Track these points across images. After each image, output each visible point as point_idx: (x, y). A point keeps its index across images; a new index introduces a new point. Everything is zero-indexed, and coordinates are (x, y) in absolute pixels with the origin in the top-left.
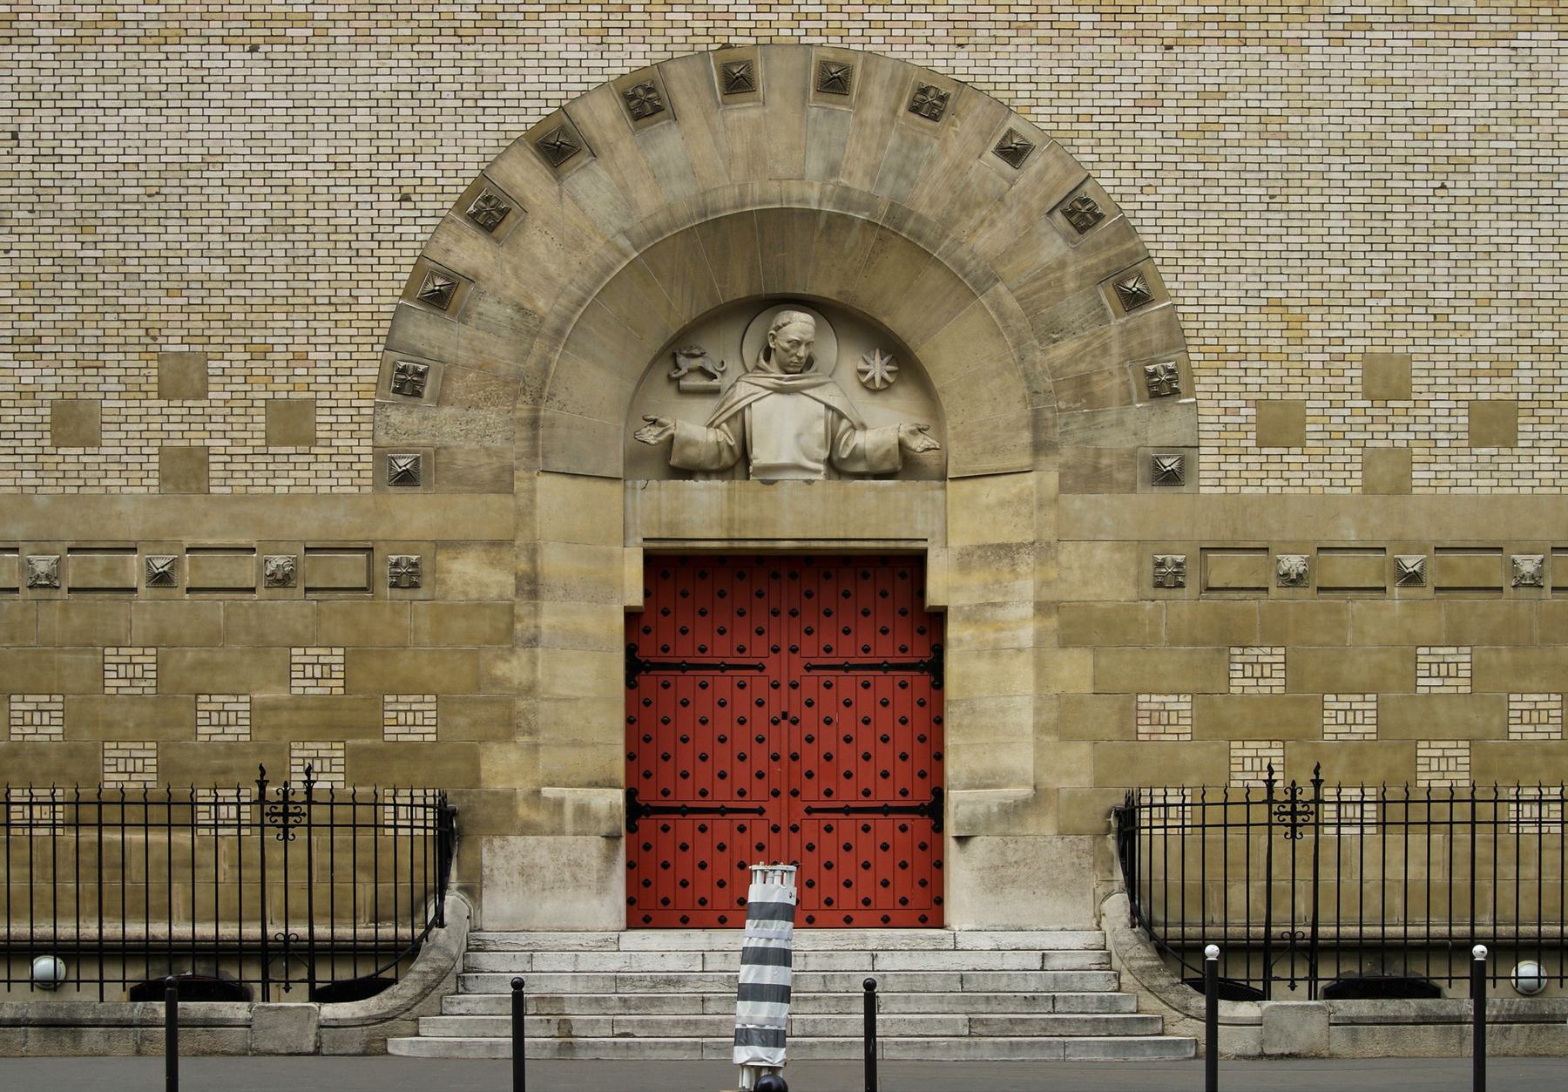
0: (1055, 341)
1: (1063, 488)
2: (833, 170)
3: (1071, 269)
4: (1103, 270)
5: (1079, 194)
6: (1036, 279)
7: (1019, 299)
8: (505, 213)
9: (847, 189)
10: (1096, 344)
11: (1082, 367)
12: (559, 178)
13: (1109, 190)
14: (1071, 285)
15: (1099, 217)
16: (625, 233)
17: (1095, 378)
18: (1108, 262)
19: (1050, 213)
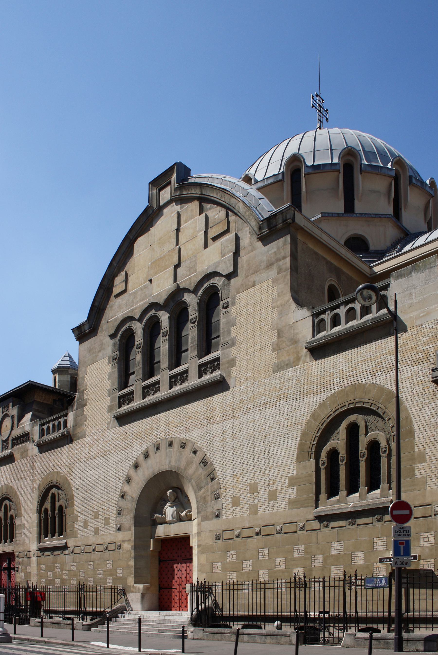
0: (200, 490)
1: (202, 521)
2: (170, 462)
3: (203, 475)
4: (208, 474)
5: (204, 459)
6: (197, 478)
7: (195, 482)
8: (130, 479)
9: (172, 465)
10: (207, 490)
11: (205, 495)
12: (136, 472)
13: (209, 456)
14: (203, 478)
15: (207, 463)
16: (144, 480)
17: (206, 497)
18: (208, 472)
19: (200, 464)
